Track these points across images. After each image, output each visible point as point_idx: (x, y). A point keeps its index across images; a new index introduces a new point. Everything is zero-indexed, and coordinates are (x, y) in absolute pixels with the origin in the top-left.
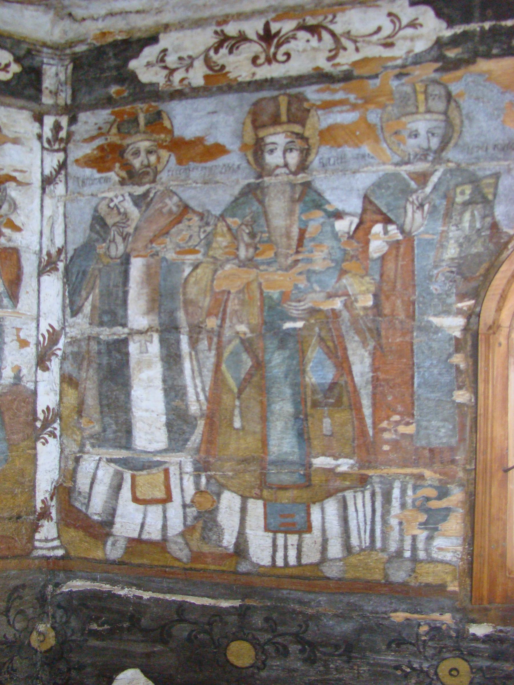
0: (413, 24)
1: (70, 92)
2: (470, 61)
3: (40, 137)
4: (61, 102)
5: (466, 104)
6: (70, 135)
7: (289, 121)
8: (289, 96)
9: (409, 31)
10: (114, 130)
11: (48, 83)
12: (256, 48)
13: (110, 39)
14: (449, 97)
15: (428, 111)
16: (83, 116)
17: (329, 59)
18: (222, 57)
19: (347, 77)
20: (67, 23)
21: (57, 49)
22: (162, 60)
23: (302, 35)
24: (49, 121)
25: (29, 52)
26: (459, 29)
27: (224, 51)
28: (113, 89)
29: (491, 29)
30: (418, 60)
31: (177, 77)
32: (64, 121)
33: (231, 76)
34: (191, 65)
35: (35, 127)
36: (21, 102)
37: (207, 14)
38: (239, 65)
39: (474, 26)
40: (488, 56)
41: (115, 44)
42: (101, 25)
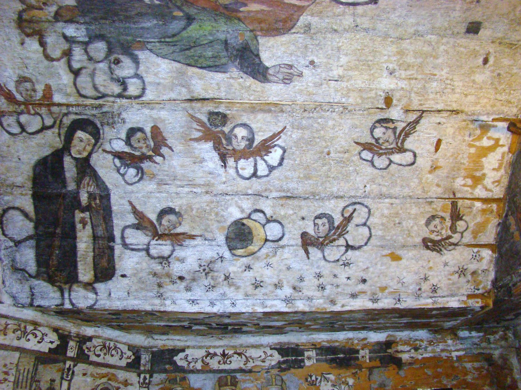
0: (271, 356)
1: (150, 365)
2: (289, 369)
3: (139, 382)
4: (147, 369)
5: (288, 383)
6: (150, 382)
7: (231, 385)
8: (231, 376)
9: (270, 358)
10: (167, 382)
11: (143, 362)
12: (220, 358)
13: (167, 348)
14: (282, 380)
15: (276, 385)
16: (155, 375)
17: (244, 364)
18: (208, 360)
19: (250, 371)
20: (150, 340)
21: (146, 348)
22: (186, 358)
23: (236, 356)
24: (142, 376)
25: (137, 350)
26: (285, 359)
27: (208, 358)
28: (167, 366)
29: (295, 359)
30: (273, 367)
31: (192, 365)
32: (148, 376)
33: (211, 367)
34: (197, 361)
35: (137, 379)
36: (134, 370)
37: (203, 344)
38: (214, 363)
39: (290, 358)
40: (294, 368)
41: (168, 350)
42: (163, 342)
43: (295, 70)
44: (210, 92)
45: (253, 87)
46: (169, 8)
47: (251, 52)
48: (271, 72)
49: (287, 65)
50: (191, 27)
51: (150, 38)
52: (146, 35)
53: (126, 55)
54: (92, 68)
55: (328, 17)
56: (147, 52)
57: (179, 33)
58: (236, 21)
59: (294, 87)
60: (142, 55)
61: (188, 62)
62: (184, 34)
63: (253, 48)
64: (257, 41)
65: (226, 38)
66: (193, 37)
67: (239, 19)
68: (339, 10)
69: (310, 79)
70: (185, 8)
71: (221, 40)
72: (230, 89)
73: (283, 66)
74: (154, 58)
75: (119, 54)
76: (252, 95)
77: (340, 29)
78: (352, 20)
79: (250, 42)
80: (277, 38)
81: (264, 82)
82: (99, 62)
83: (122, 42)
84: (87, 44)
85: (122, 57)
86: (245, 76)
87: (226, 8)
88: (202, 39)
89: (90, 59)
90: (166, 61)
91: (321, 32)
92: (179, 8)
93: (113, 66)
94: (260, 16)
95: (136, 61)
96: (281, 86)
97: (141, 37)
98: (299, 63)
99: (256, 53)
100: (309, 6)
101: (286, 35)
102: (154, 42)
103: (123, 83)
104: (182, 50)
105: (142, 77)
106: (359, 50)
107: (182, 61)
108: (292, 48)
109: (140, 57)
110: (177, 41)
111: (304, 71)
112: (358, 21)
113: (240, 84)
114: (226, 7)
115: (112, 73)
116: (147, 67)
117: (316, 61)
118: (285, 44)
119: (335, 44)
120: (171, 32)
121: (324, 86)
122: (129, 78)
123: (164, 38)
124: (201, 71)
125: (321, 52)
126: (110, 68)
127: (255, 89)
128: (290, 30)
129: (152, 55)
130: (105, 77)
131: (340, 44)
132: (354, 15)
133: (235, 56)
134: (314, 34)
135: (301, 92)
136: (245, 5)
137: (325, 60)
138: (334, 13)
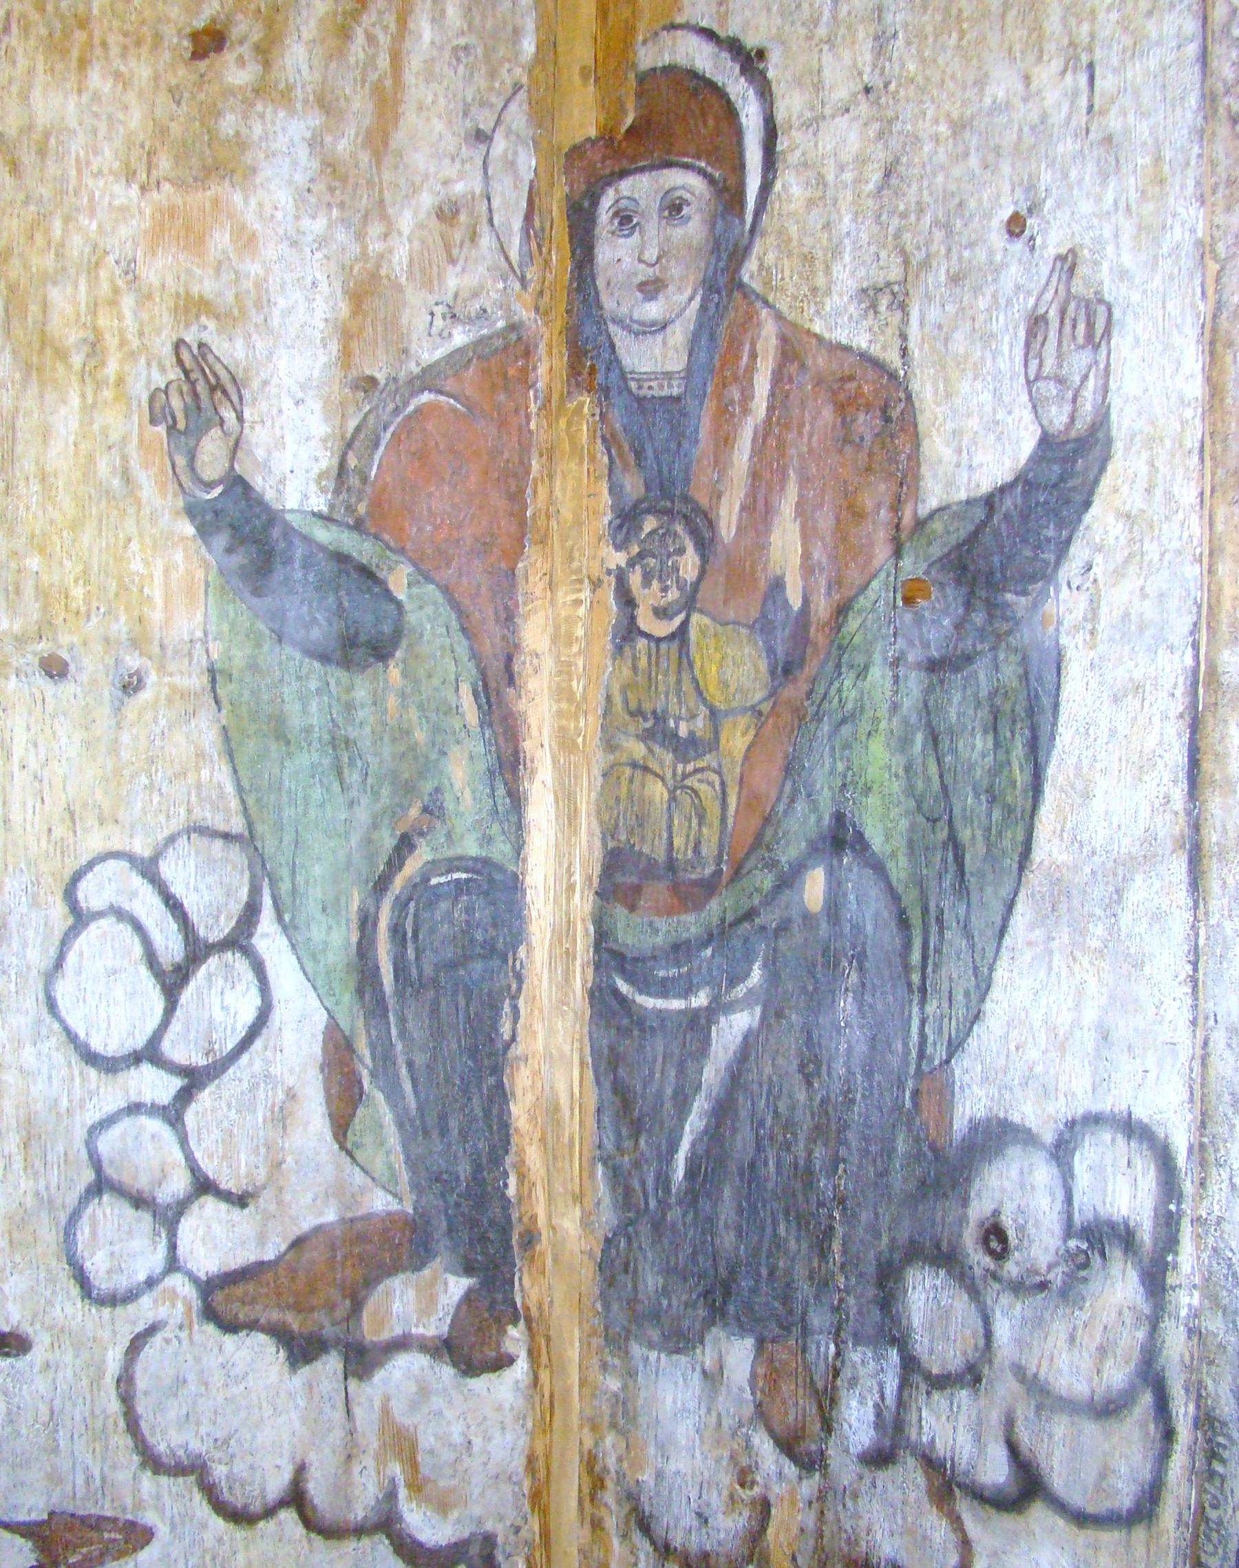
43: (1049, 295)
44: (1151, 742)
45: (1134, 500)
46: (783, 927)
47: (974, 537)
48: (1058, 417)
49: (1028, 345)
50: (868, 833)
51: (906, 1045)
52: (895, 1062)
53: (968, 1180)
54: (1014, 1384)
55: (827, 226)
56: (959, 1067)
57: (894, 896)
58: (853, 624)
59: (1123, 274)
60: (971, 1104)
61: (1011, 862)
62: (899, 870)
63: (963, 530)
64: (931, 515)
65: (919, 665)
66: (913, 827)
67: (842, 610)
68: (796, 190)
69: (1086, 207)
70: (788, 854)
71: (929, 690)
72: (1142, 629)
73: (1033, 365)
74: (987, 1038)
75: (963, 1219)
76: (1169, 496)
77: (881, 155)
78: (842, 122)
79: (936, 551)
80: (923, 421)
81: (1109, 442)
82: (988, 1335)
83: (912, 1186)
84: (910, 1364)
85: (979, 1209)
86: (1078, 552)
87: (787, 671)
88: (920, 785)
89: (972, 1375)
90: (1000, 974)
91: (897, 237)
92: (789, 880)
93: (1011, 1268)
94: (825, 521)
95: (995, 1136)
96: (1121, 343)
97: (901, 1086)
98: (1018, 288)
99: (979, 513)
100: (779, 317)
101: (915, 386)
102: (923, 1022)
103: (1098, 1238)
104: (961, 888)
105: (1071, 1124)
106: (962, 34)
107: (1005, 891)
108: (959, 343)
109: (981, 1113)
110: (925, 910)
111: (1052, 251)
112: (841, 94)
113: (1118, 574)
114: (785, 670)
115: (1043, 1286)
116: (1025, 1084)
117: (1006, 214)
118: (946, 381)
119: (942, 157)
120: (889, 937)
121: (1113, 122)
122: (1069, 1199)
123: (907, 968)
124: (1050, 794)
125: (972, 204)
126: (1017, 1288)
127: (1141, 483)
128: (893, 376)
129: (972, 1043)
130: (1059, 1329)
131: (943, 129)
132: (813, 123)
133: (991, 616)
134: (906, 263)
135: (1150, 232)
136: (778, 585)
137: (1006, 169)
138: (810, 203)
